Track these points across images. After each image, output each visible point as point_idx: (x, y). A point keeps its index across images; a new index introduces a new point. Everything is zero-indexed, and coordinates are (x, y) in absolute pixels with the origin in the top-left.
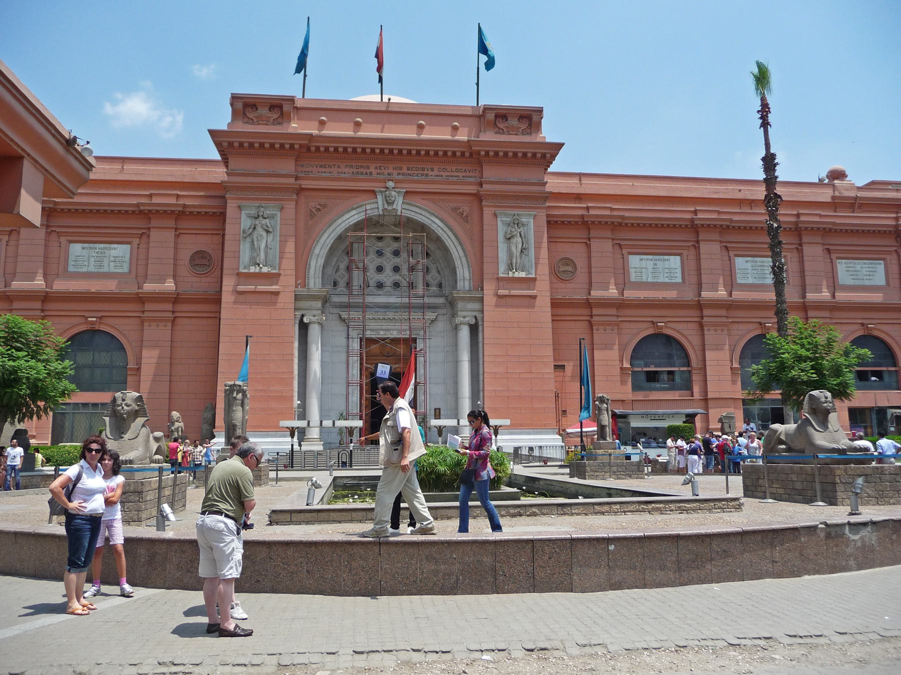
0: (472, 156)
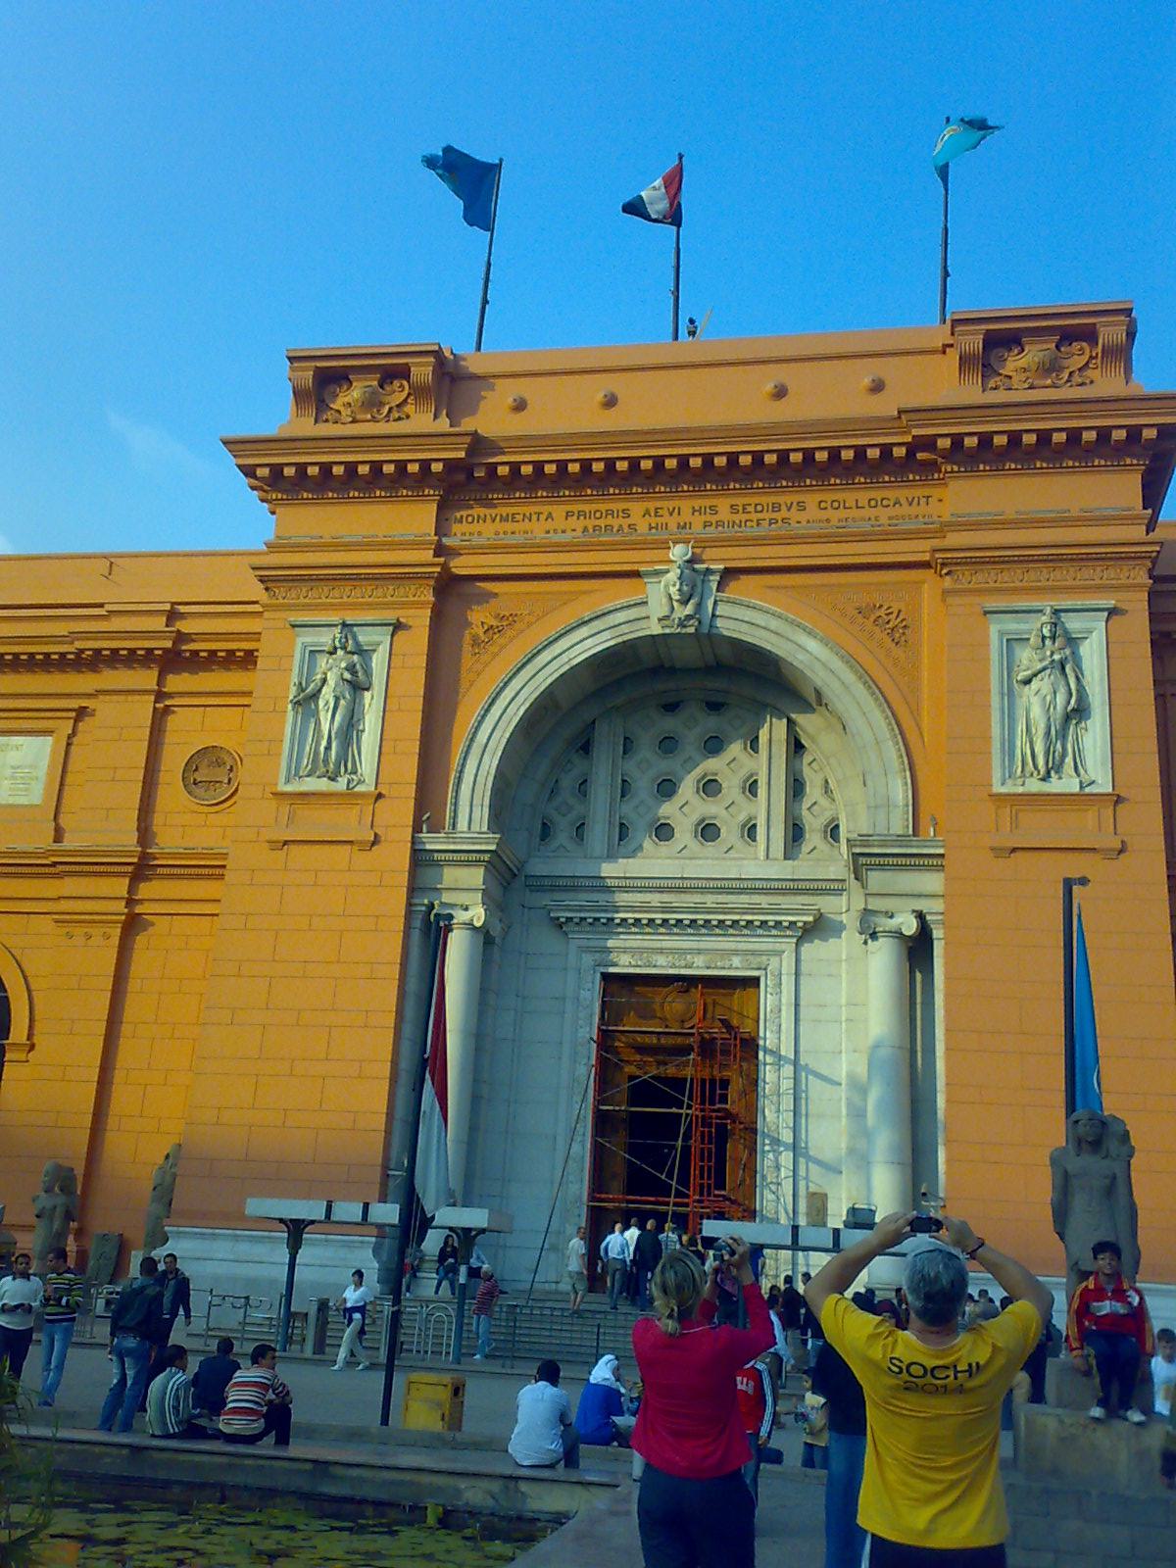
0: (915, 457)
